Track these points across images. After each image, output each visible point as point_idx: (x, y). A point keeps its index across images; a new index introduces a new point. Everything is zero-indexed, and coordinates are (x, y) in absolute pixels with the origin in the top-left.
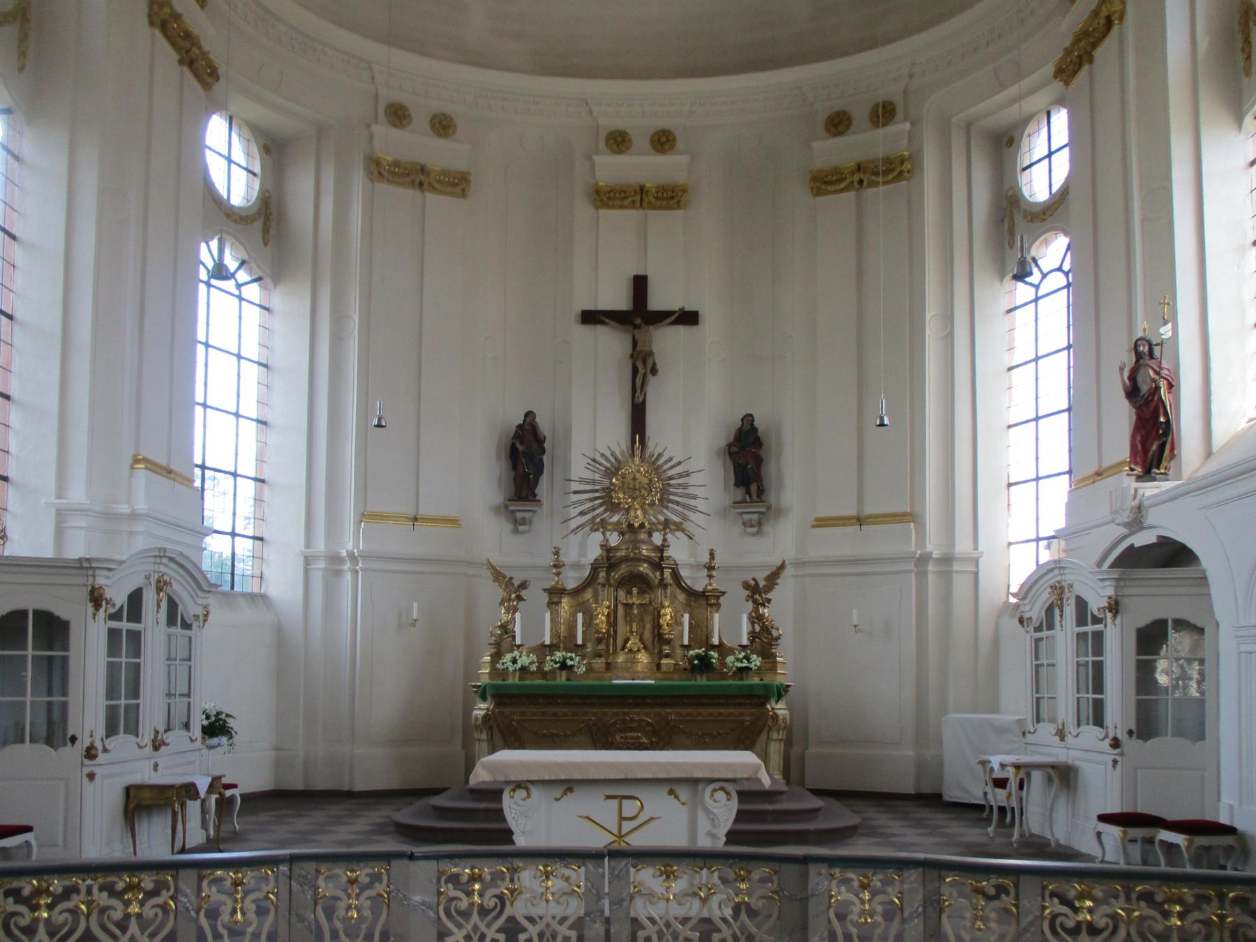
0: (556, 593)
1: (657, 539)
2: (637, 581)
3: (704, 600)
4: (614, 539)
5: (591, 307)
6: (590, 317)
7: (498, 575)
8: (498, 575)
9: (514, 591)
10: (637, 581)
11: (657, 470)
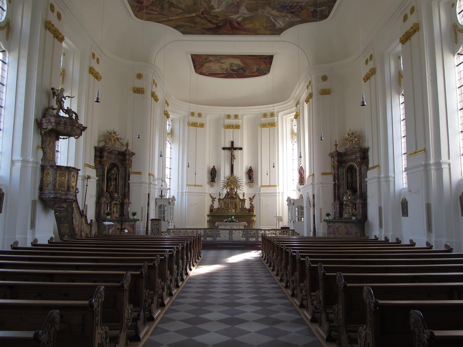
0: (219, 200)
2: (232, 198)
6: (224, 149)
9: (213, 199)
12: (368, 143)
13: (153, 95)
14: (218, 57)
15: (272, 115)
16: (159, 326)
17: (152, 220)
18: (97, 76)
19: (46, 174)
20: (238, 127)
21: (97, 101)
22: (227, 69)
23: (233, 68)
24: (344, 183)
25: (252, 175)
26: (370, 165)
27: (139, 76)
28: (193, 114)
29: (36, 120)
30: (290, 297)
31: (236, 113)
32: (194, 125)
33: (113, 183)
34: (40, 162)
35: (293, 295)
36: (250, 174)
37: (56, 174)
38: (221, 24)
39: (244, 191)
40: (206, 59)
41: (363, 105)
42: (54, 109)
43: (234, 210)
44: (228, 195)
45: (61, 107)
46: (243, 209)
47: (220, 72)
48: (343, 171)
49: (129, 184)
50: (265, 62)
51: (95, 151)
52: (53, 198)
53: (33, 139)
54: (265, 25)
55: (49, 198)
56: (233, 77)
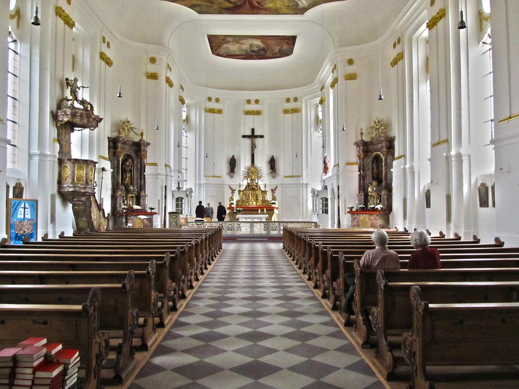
0: (240, 191)
1: (256, 182)
2: (253, 189)
3: (264, 192)
4: (249, 182)
5: (244, 134)
6: (244, 136)
7: (231, 188)
8: (231, 188)
9: (233, 191)
10: (253, 189)
11: (256, 169)
12: (395, 132)
13: (168, 81)
14: (237, 38)
15: (296, 100)
16: (191, 302)
17: (170, 213)
18: (109, 63)
19: (64, 168)
20: (258, 113)
21: (120, 96)
22: (246, 50)
23: (253, 49)
24: (369, 173)
25: (275, 164)
26: (396, 155)
27: (153, 60)
28: (210, 99)
29: (52, 112)
30: (306, 281)
31: (257, 98)
32: (212, 111)
33: (128, 175)
34: (57, 156)
35: (309, 279)
36: (272, 163)
37: (74, 167)
38: (239, 3)
39: (264, 181)
40: (223, 40)
41: (381, 99)
42: (68, 100)
43: (254, 203)
44: (249, 187)
45: (76, 99)
46: (264, 201)
47: (240, 54)
48: (369, 160)
49: (144, 176)
50: (288, 43)
51: (109, 142)
52: (72, 191)
53: (51, 131)
54: (287, 5)
55: (68, 191)
56: (255, 59)
